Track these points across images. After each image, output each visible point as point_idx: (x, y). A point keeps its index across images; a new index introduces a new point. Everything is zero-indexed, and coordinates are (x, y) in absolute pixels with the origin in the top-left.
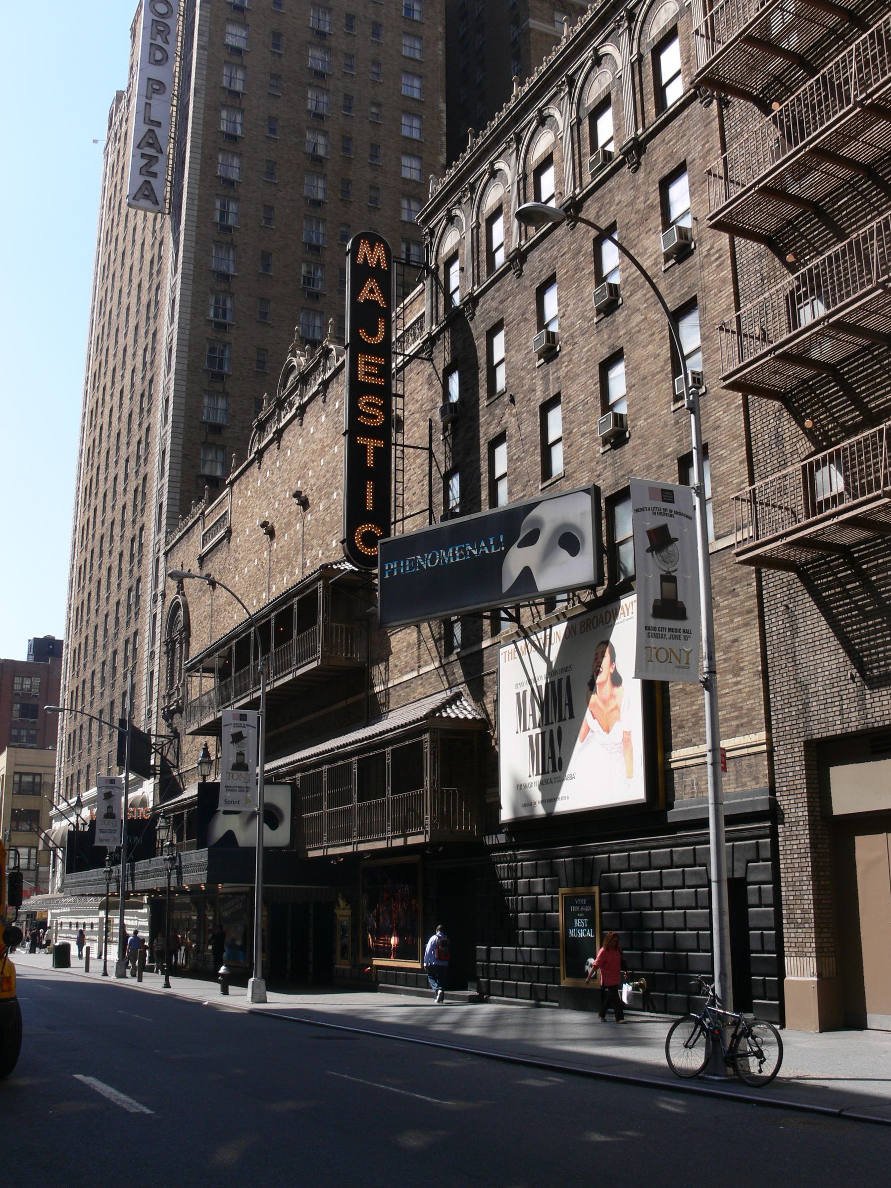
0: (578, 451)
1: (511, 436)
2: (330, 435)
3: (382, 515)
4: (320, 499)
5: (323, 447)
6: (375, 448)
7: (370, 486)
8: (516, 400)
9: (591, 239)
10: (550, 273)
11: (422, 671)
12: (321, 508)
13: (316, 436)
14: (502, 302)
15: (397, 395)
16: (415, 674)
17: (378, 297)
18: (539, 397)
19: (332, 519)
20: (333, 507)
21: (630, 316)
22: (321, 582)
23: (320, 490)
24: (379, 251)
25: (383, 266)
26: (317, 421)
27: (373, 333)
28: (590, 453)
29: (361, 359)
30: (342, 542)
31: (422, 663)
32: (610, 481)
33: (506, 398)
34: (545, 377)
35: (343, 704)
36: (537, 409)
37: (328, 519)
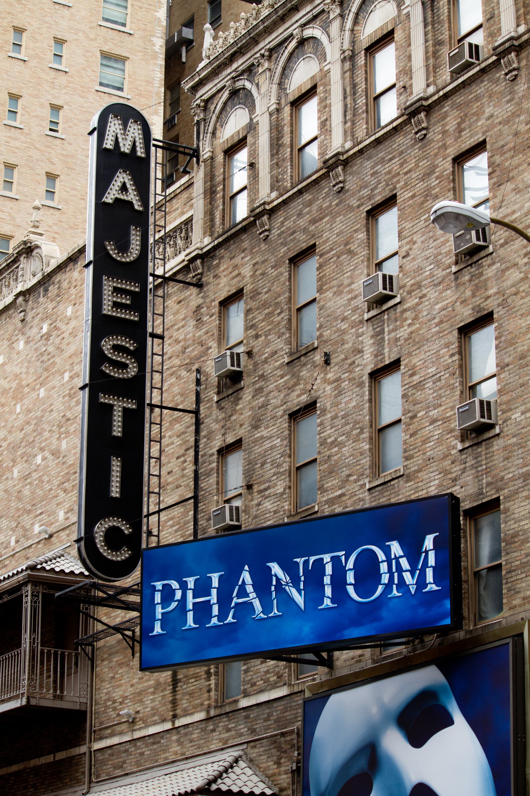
0: (424, 442)
1: (324, 411)
2: (32, 370)
3: (131, 504)
4: (14, 461)
5: (20, 387)
6: (125, 409)
7: (116, 466)
8: (333, 361)
9: (450, 159)
10: (387, 194)
11: (178, 723)
12: (16, 474)
13: (8, 368)
14: (314, 221)
15: (153, 336)
16: (168, 726)
17: (132, 196)
18: (367, 362)
19: (33, 493)
20: (35, 475)
21: (504, 271)
22: (29, 588)
23: (14, 447)
24: (135, 131)
25: (140, 152)
26: (11, 347)
27: (124, 248)
28: (443, 448)
29: (108, 286)
30: (78, 541)
31: (179, 711)
32: (472, 489)
33: (318, 358)
34: (379, 335)
35: (50, 758)
36: (366, 378)
37: (26, 492)
